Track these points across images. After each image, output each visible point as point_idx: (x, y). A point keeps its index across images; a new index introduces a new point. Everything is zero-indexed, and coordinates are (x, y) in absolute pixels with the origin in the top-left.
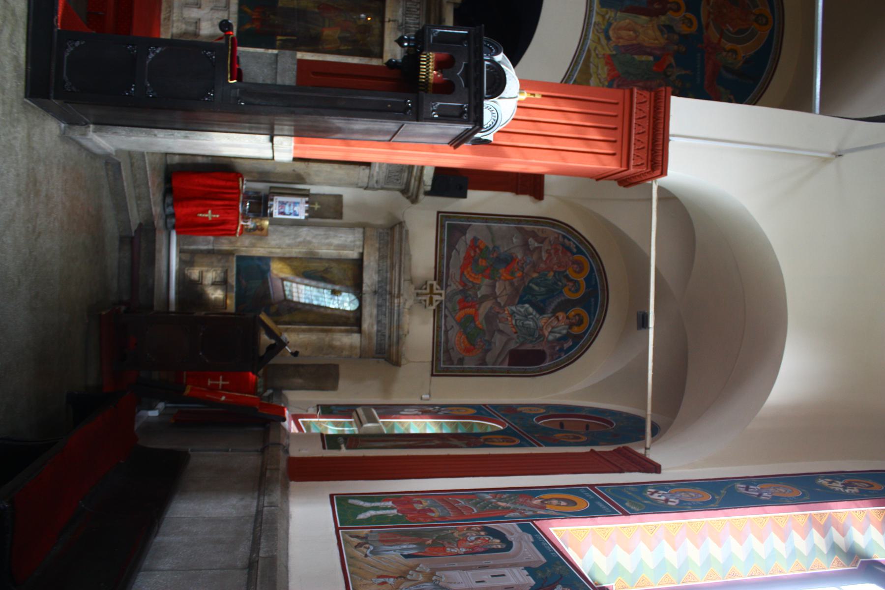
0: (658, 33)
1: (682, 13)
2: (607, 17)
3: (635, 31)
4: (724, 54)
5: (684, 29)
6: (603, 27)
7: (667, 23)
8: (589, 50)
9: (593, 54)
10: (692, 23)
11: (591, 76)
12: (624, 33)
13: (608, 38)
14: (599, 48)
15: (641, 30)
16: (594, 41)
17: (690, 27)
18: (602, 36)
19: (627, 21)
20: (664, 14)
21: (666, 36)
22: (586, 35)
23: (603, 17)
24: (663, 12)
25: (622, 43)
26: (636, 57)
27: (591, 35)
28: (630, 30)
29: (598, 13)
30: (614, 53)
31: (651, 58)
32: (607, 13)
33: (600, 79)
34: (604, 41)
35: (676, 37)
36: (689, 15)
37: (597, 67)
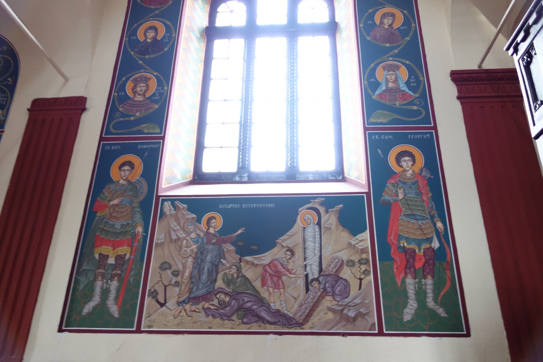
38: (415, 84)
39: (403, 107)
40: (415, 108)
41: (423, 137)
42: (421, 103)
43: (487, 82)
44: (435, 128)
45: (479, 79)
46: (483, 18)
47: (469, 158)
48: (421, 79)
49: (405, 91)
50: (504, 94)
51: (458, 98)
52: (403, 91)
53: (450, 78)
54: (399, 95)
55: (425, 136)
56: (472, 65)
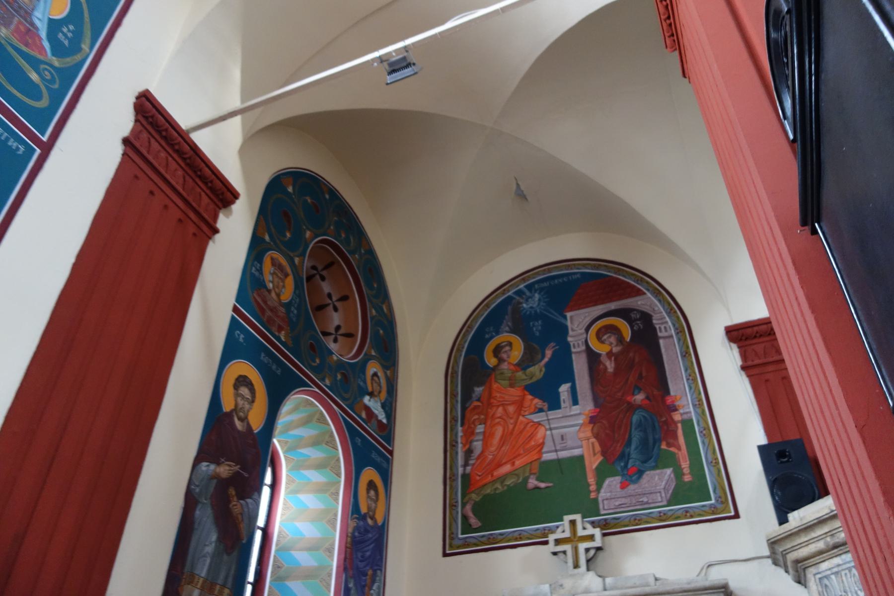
38: (66, 43)
39: (10, 49)
40: (34, 76)
41: (7, 139)
42: (52, 81)
43: (183, 165)
44: (47, 148)
45: (177, 147)
46: (236, 74)
47: (72, 260)
48: (85, 47)
49: (37, 29)
50: (194, 204)
51: (126, 141)
52: (32, 24)
53: (133, 100)
54: (20, 23)
55: (12, 143)
56: (183, 114)
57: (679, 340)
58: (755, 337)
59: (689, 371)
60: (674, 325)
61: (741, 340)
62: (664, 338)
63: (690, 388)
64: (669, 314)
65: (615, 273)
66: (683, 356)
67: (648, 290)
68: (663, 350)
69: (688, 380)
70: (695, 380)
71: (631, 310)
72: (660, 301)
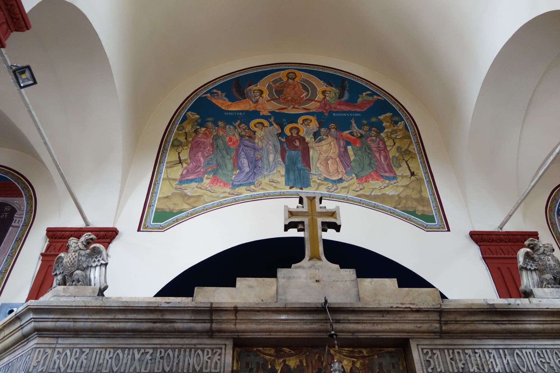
0: (323, 143)
1: (299, 125)
2: (318, 181)
3: (327, 160)
4: (327, 98)
5: (314, 125)
6: (330, 185)
7: (311, 136)
8: (358, 196)
9: (360, 192)
10: (308, 119)
11: (384, 194)
12: (332, 168)
13: (341, 180)
14: (354, 187)
15: (325, 155)
16: (348, 192)
17: (311, 121)
18: (340, 185)
19: (318, 165)
20: (304, 139)
21: (324, 137)
22: (344, 199)
23: (319, 185)
24: (302, 140)
25: (341, 169)
26: (352, 159)
27: (343, 194)
28: (327, 163)
29: (317, 189)
30: (354, 175)
31: (349, 148)
32: (314, 181)
33: (385, 187)
34: (345, 184)
35: (323, 130)
36: (300, 120)
37: (374, 189)
57: (22, 230)
58: (61, 238)
59: (14, 250)
60: (25, 220)
61: (52, 238)
62: (14, 226)
63: (7, 261)
64: (27, 212)
65: (15, 180)
66: (17, 240)
67: (26, 195)
68: (8, 234)
69: (9, 255)
70: (12, 257)
71: (7, 205)
72: (28, 203)
